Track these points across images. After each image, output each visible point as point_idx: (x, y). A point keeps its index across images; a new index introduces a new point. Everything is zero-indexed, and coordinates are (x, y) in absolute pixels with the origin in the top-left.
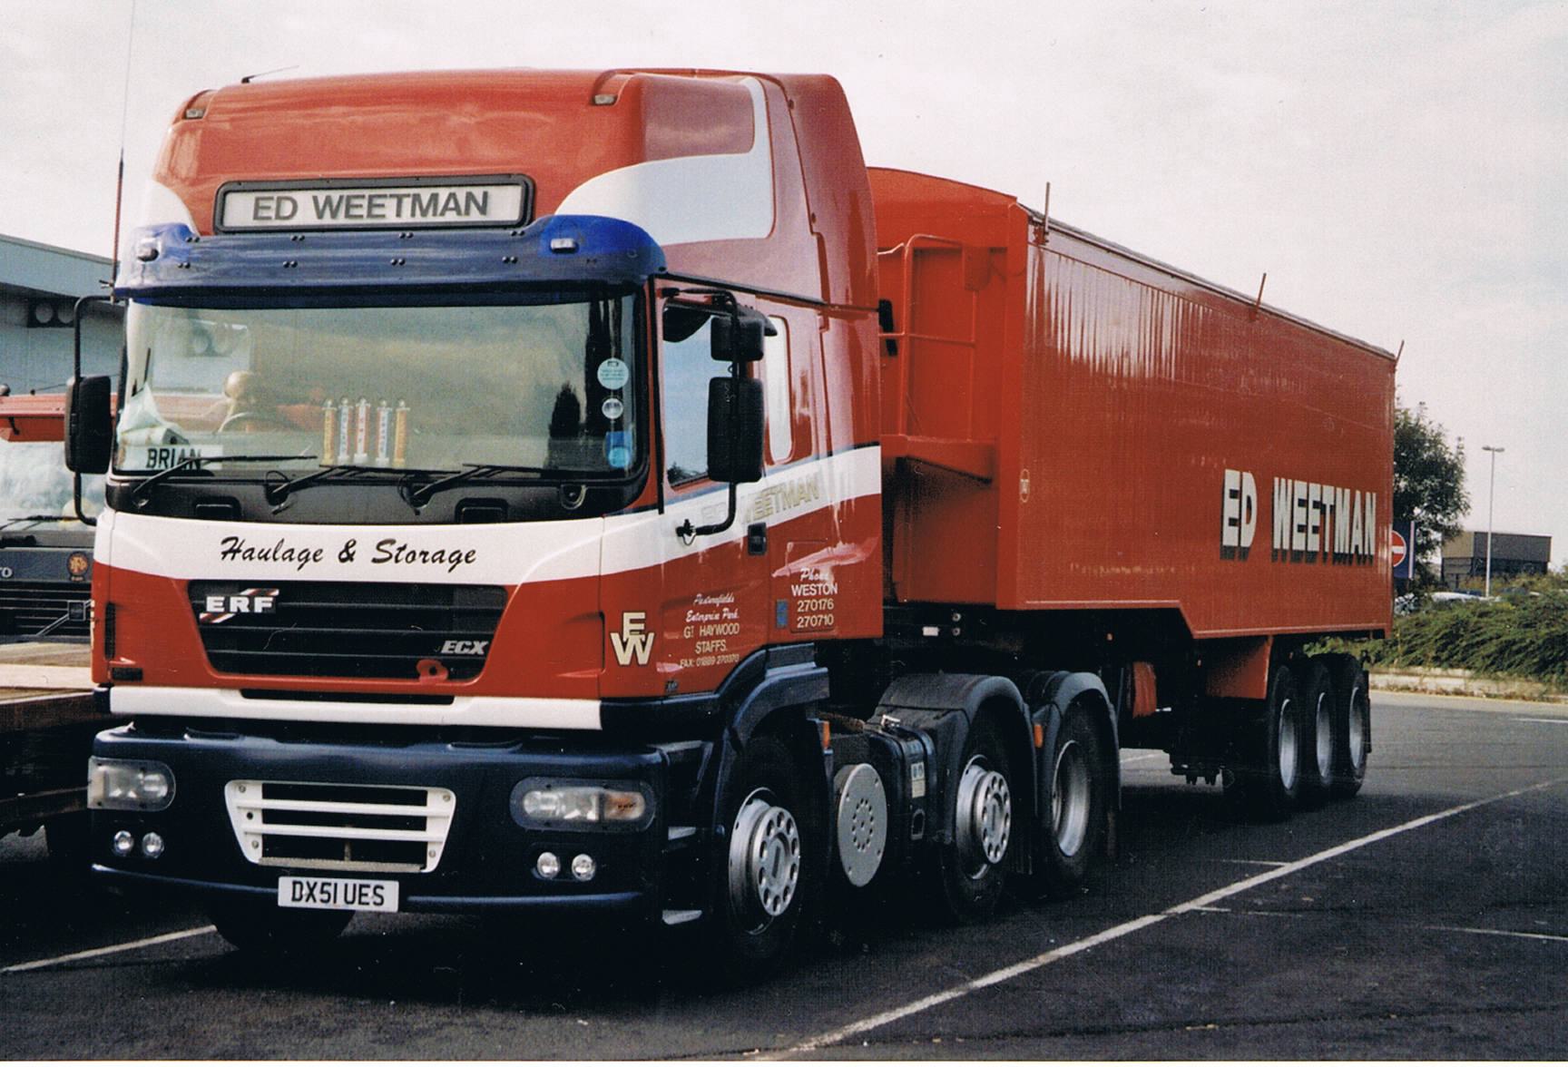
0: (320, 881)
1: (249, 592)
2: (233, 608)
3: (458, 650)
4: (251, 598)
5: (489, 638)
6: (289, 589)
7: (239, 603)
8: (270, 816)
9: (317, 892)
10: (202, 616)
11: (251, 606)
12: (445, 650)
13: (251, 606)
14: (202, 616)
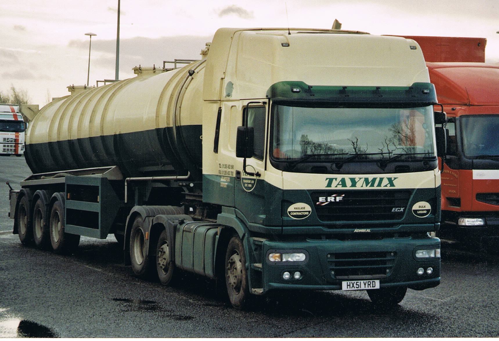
0: (355, 282)
1: (334, 195)
2: (329, 200)
3: (396, 211)
4: (335, 197)
5: (406, 207)
6: (347, 193)
7: (331, 199)
8: (337, 264)
9: (355, 285)
10: (317, 203)
11: (335, 199)
12: (393, 211)
13: (335, 199)
14: (317, 203)
